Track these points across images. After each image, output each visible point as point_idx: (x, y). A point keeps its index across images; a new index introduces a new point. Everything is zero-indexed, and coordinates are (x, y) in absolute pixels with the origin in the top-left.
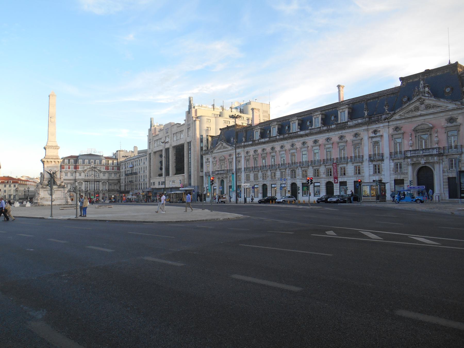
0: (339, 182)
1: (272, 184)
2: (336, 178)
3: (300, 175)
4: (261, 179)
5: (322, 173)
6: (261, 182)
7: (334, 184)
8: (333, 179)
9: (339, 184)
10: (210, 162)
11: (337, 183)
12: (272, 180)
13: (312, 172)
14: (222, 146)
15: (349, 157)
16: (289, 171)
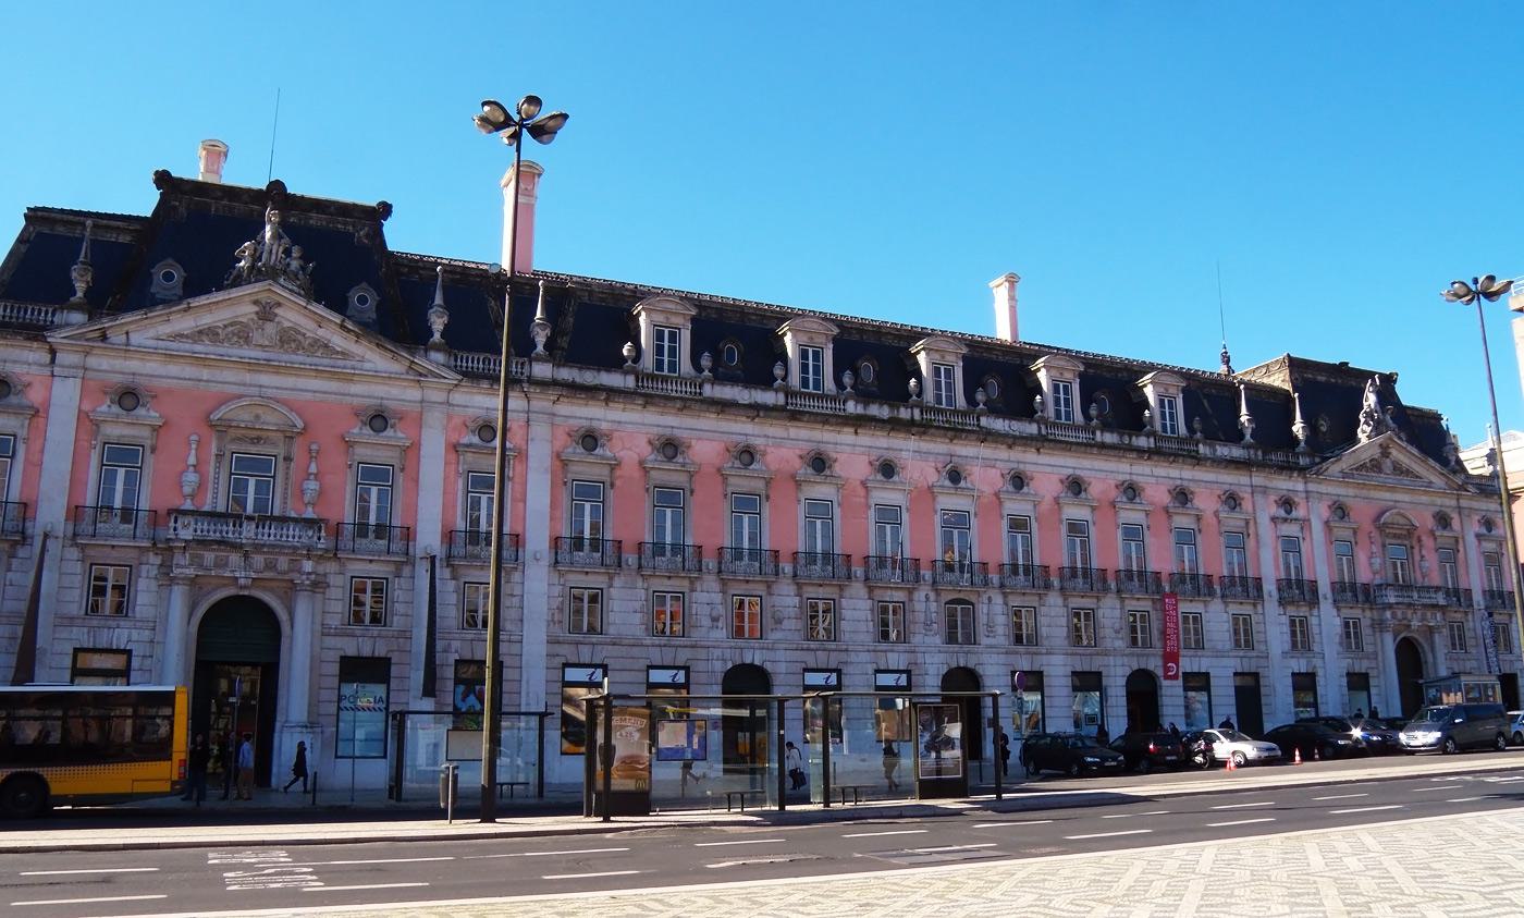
0: (1180, 674)
1: (810, 666)
2: (1171, 657)
3: (1000, 630)
4: (721, 634)
5: (1108, 632)
6: (717, 653)
7: (1165, 683)
8: (1160, 662)
9: (1181, 679)
10: (37, 413)
11: (1175, 677)
12: (813, 645)
13: (1064, 621)
14: (270, 328)
15: (785, 551)
16: (933, 606)
